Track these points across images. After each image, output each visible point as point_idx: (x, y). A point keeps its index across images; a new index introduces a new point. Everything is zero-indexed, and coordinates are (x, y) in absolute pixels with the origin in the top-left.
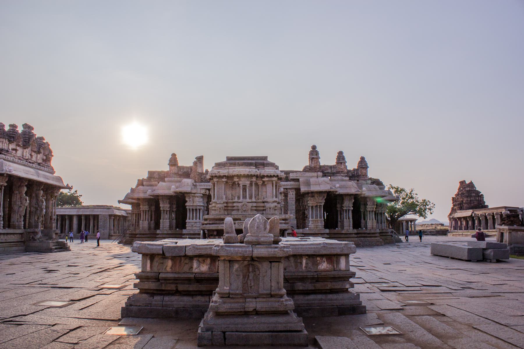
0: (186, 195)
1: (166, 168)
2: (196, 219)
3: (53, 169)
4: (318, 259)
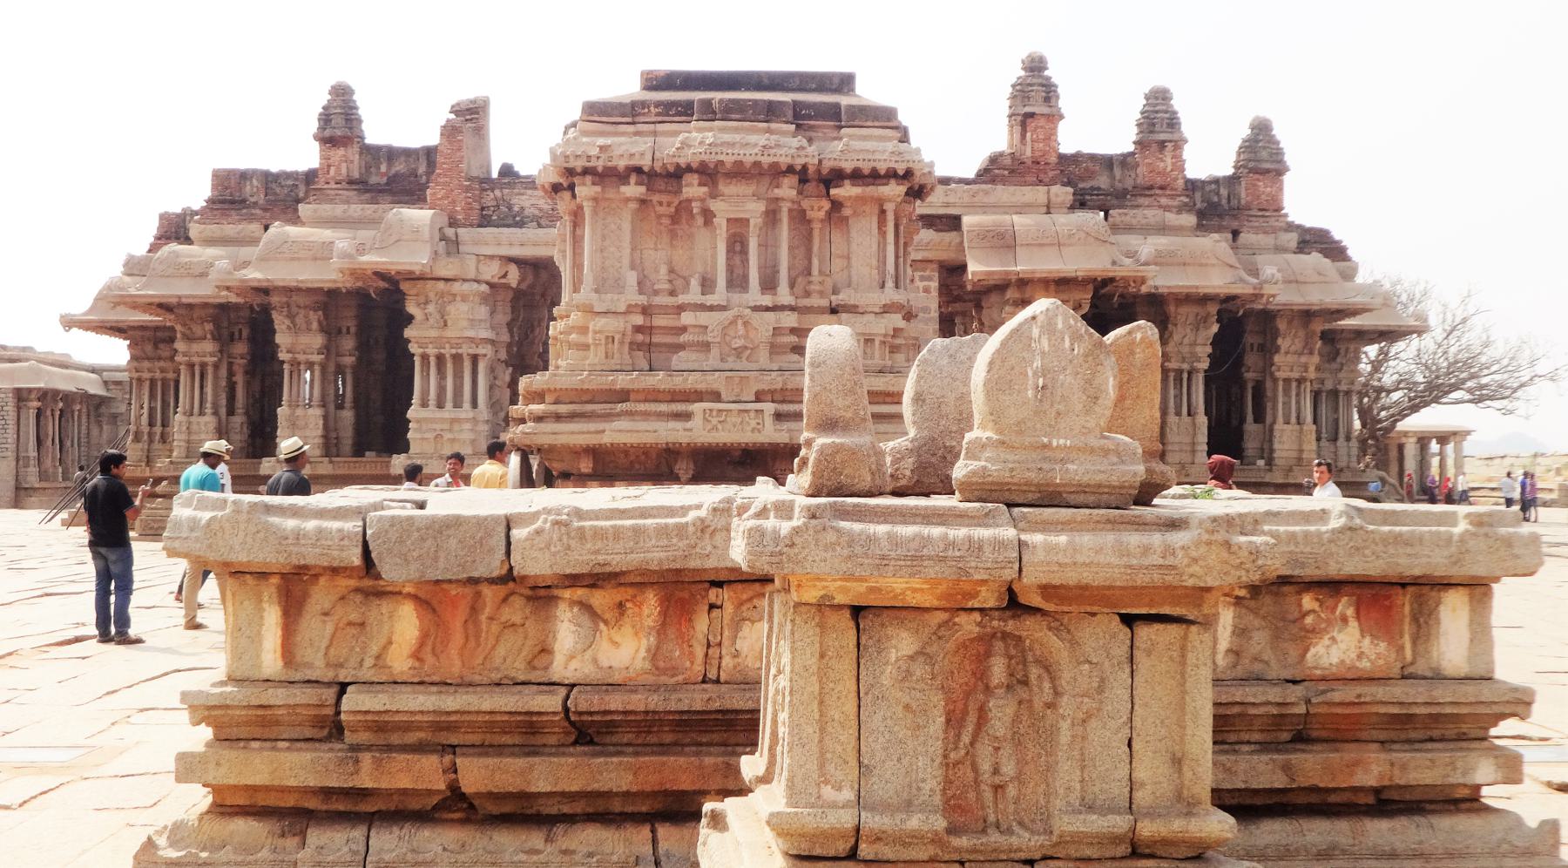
0: (404, 286)
1: (299, 153)
2: (457, 404)
4: (1308, 601)
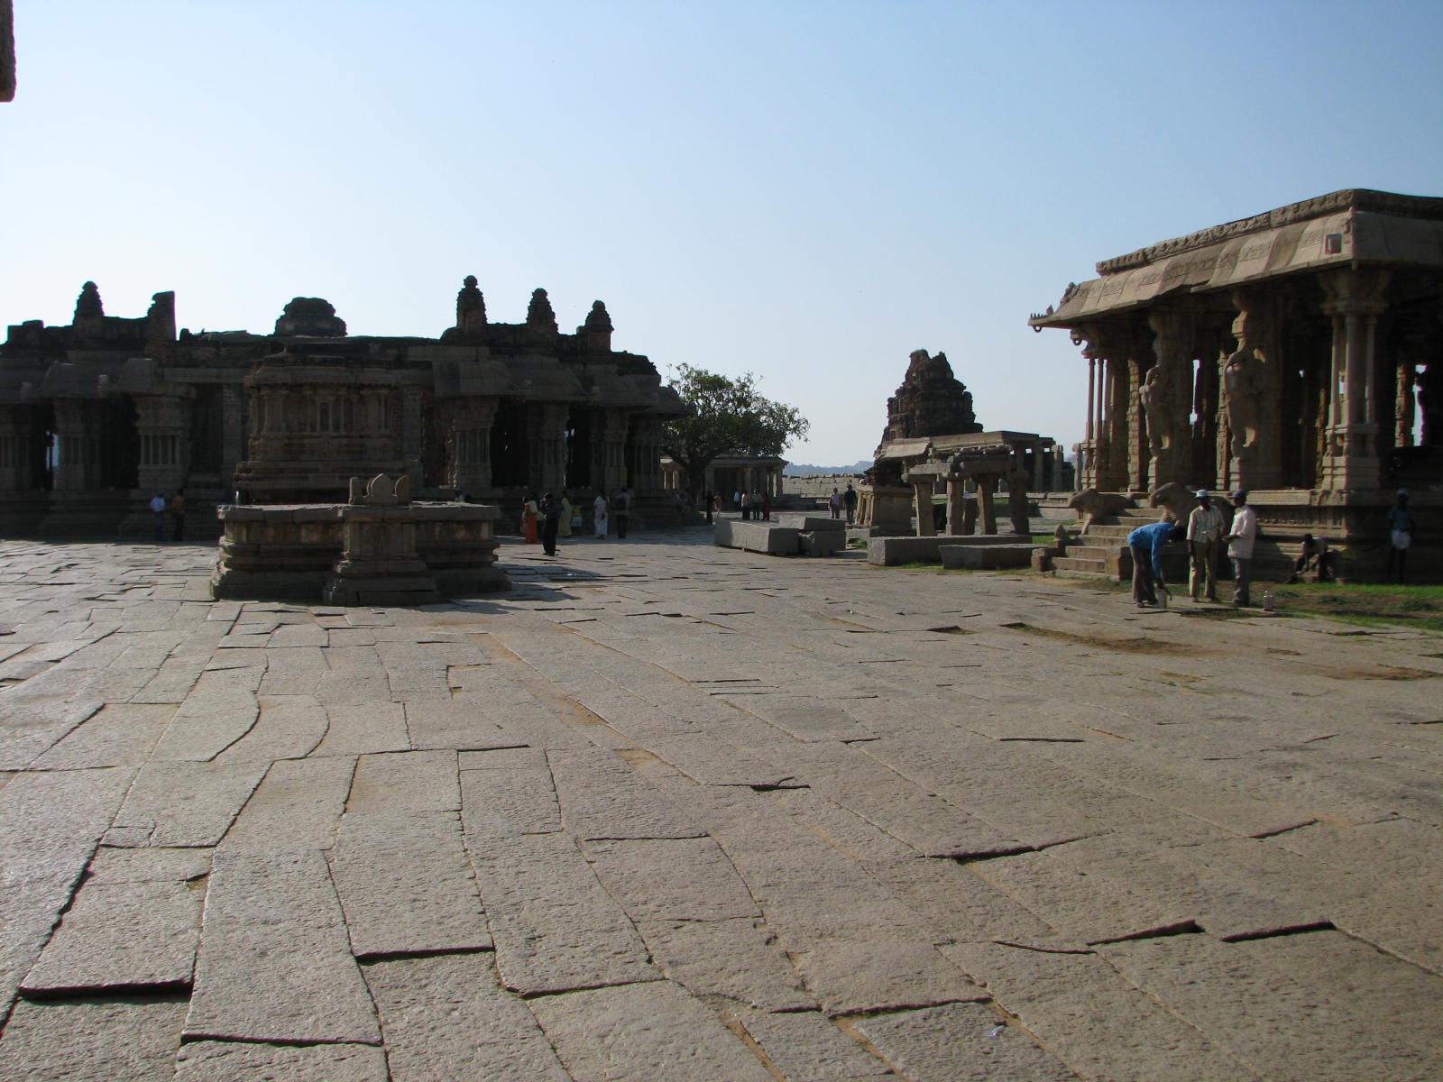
1: (60, 314)
2: (165, 462)
4: (455, 525)
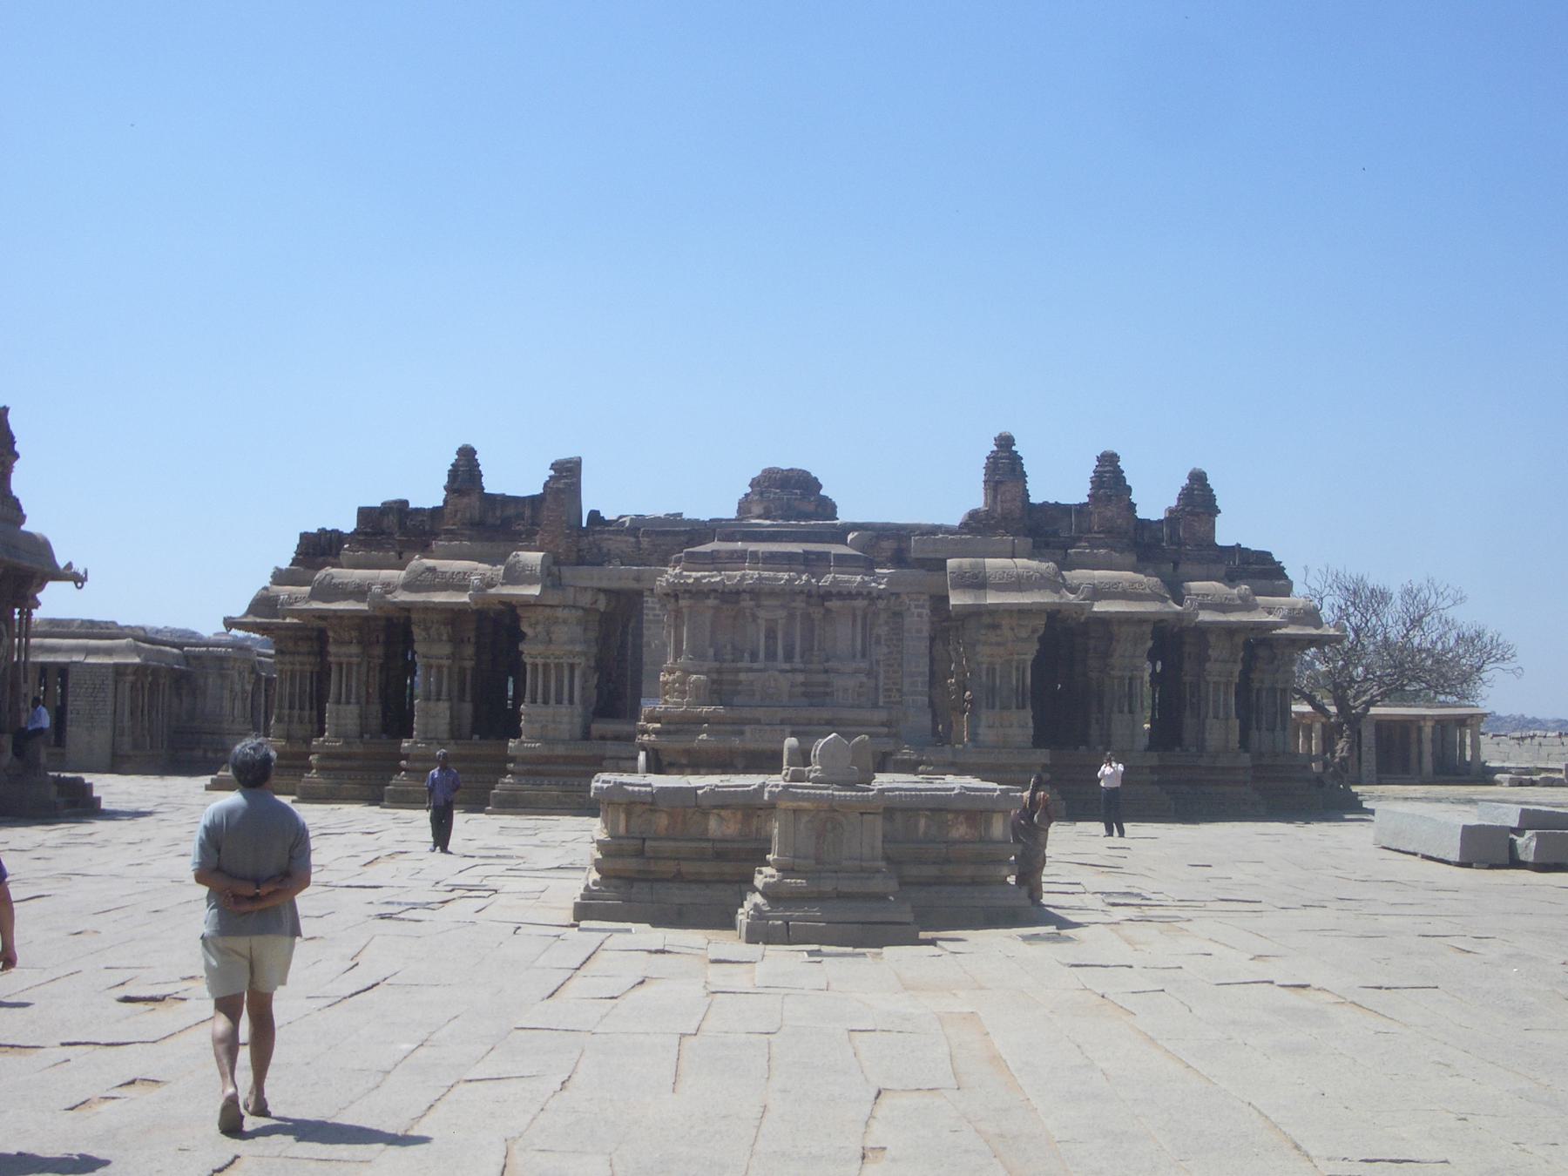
0: (519, 611)
1: (428, 493)
3: (19, 509)
4: (950, 816)
